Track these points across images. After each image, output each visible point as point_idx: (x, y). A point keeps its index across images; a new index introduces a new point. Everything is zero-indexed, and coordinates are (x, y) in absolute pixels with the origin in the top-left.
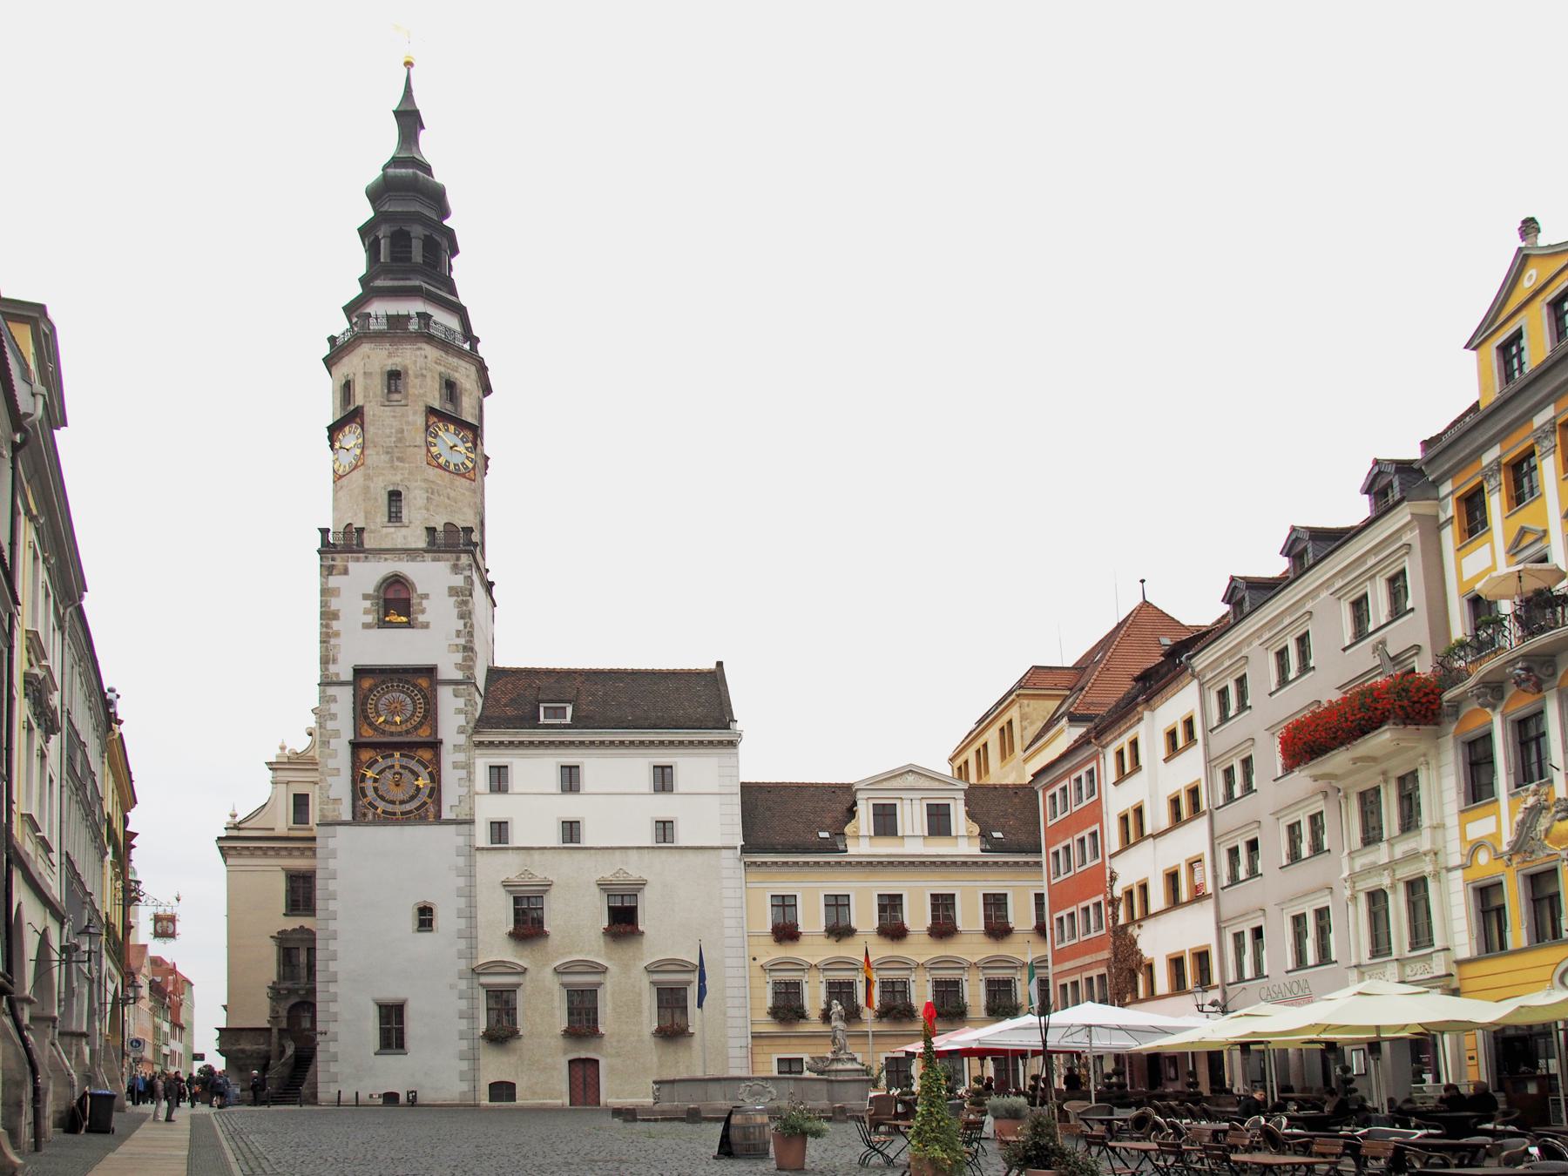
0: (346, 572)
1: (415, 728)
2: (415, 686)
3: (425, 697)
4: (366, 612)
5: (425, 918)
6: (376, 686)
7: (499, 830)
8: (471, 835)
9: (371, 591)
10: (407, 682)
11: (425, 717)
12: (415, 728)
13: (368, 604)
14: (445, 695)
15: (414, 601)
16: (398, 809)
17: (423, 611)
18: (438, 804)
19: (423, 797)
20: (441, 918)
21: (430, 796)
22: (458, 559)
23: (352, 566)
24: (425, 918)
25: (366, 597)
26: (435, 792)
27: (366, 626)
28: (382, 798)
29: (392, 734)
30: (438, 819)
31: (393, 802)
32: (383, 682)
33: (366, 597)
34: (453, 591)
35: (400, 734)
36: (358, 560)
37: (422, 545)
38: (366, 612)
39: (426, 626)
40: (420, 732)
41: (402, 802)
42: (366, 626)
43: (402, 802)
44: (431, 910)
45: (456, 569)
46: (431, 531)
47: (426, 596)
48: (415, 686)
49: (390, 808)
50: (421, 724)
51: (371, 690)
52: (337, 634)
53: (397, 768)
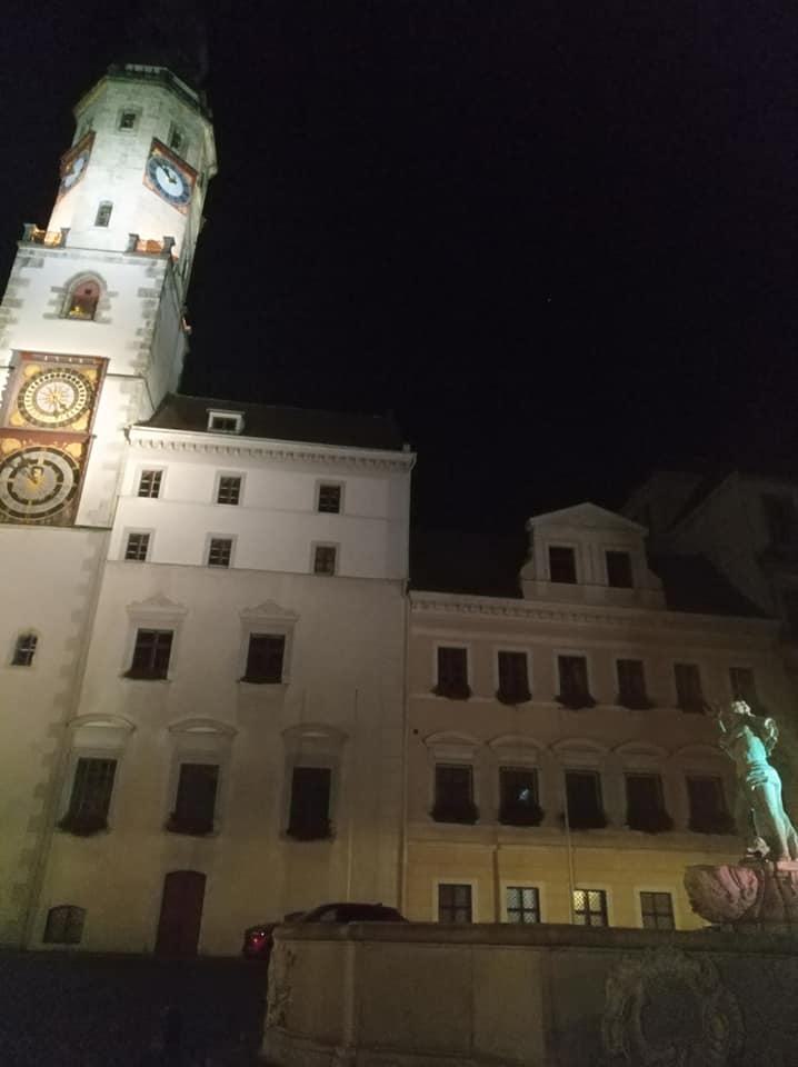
0: (41, 265)
1: (71, 421)
2: (81, 377)
3: (89, 389)
4: (52, 303)
5: (24, 651)
6: (41, 374)
7: (137, 547)
8: (103, 550)
9: (61, 284)
10: (75, 373)
11: (84, 410)
12: (71, 421)
13: (55, 296)
14: (110, 388)
15: (101, 299)
16: (29, 509)
17: (108, 308)
18: (75, 507)
19: (61, 498)
20: (42, 654)
21: (68, 498)
22: (154, 264)
23: (48, 261)
24: (24, 651)
25: (54, 289)
26: (75, 493)
27: (48, 316)
28: (15, 496)
29: (43, 425)
30: (71, 523)
31: (25, 502)
32: (50, 371)
33: (54, 289)
34: (143, 292)
35: (53, 425)
36: (55, 255)
37: (124, 249)
38: (52, 303)
39: (107, 321)
40: (74, 425)
41: (36, 503)
42: (48, 316)
43: (36, 503)
44: (35, 640)
45: (151, 272)
46: (135, 239)
47: (114, 294)
48: (81, 377)
49: (20, 508)
50: (78, 417)
51: (34, 378)
52: (14, 321)
53: (40, 463)
